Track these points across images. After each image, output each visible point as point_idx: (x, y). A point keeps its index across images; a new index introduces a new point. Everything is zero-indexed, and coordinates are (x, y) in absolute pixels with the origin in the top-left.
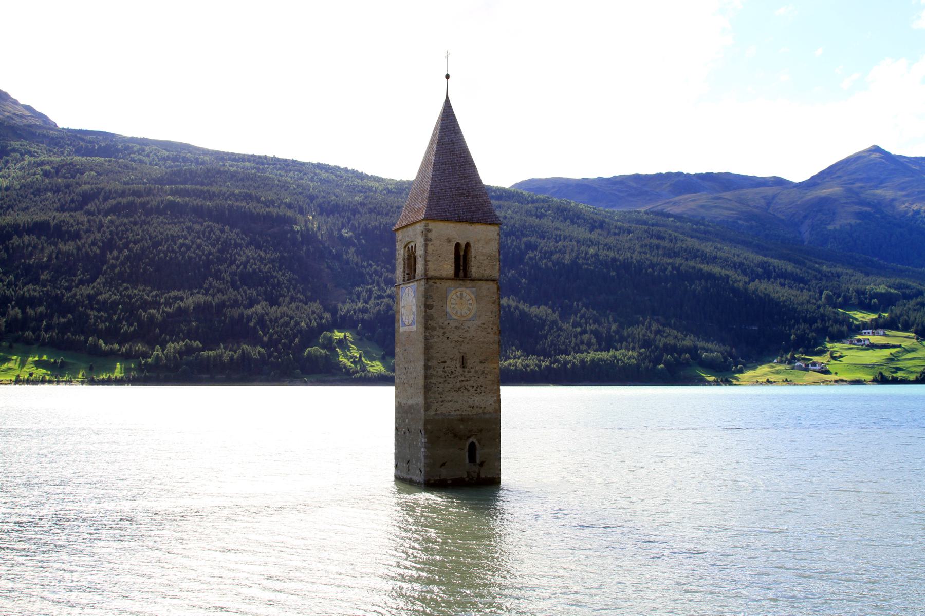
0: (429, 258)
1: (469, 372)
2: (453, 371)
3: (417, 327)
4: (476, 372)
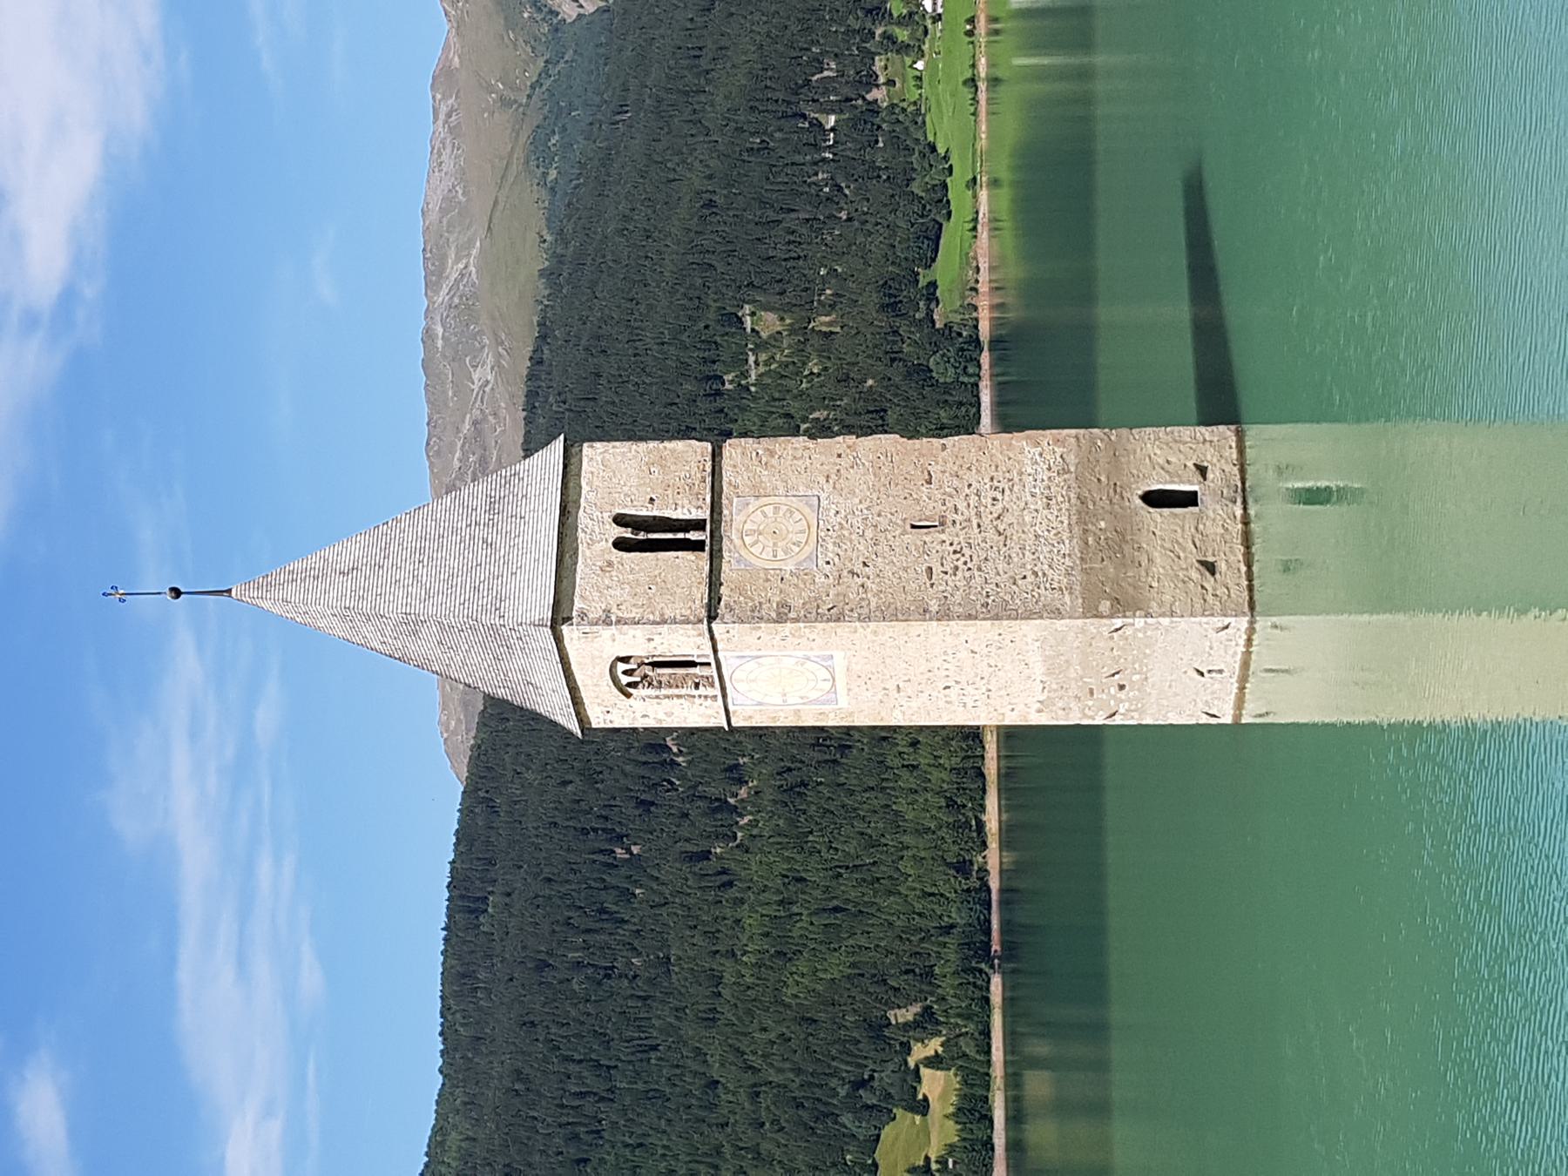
2: (951, 549)
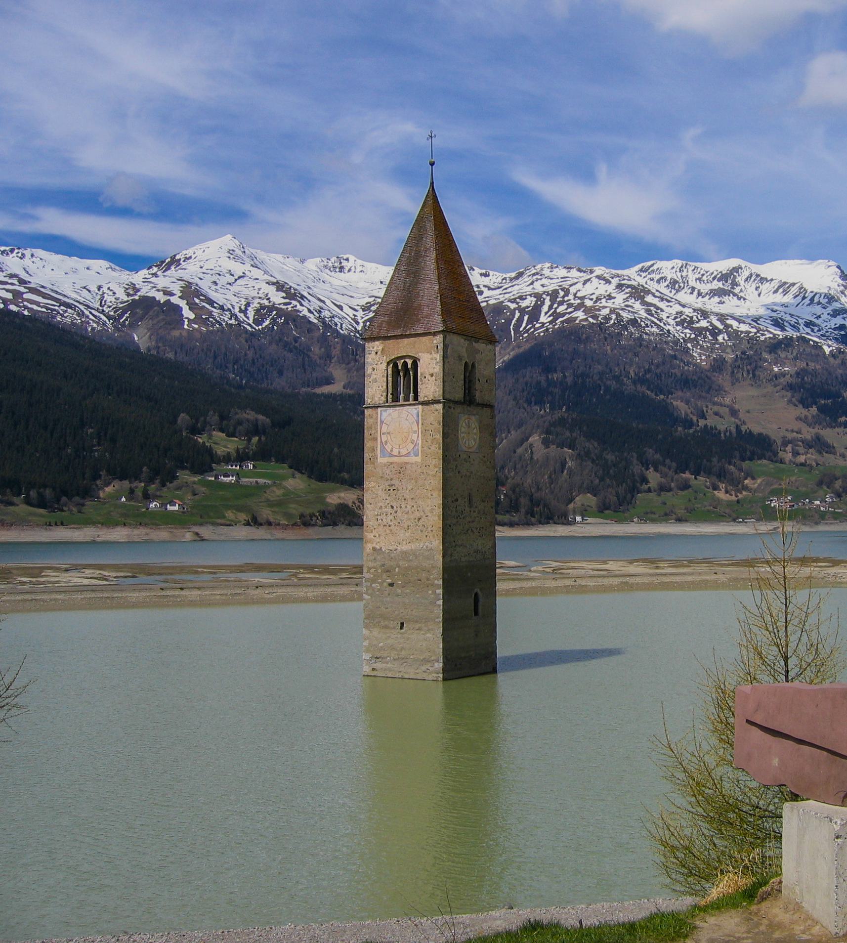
0: (446, 379)
1: (474, 512)
3: (422, 460)
4: (479, 513)
